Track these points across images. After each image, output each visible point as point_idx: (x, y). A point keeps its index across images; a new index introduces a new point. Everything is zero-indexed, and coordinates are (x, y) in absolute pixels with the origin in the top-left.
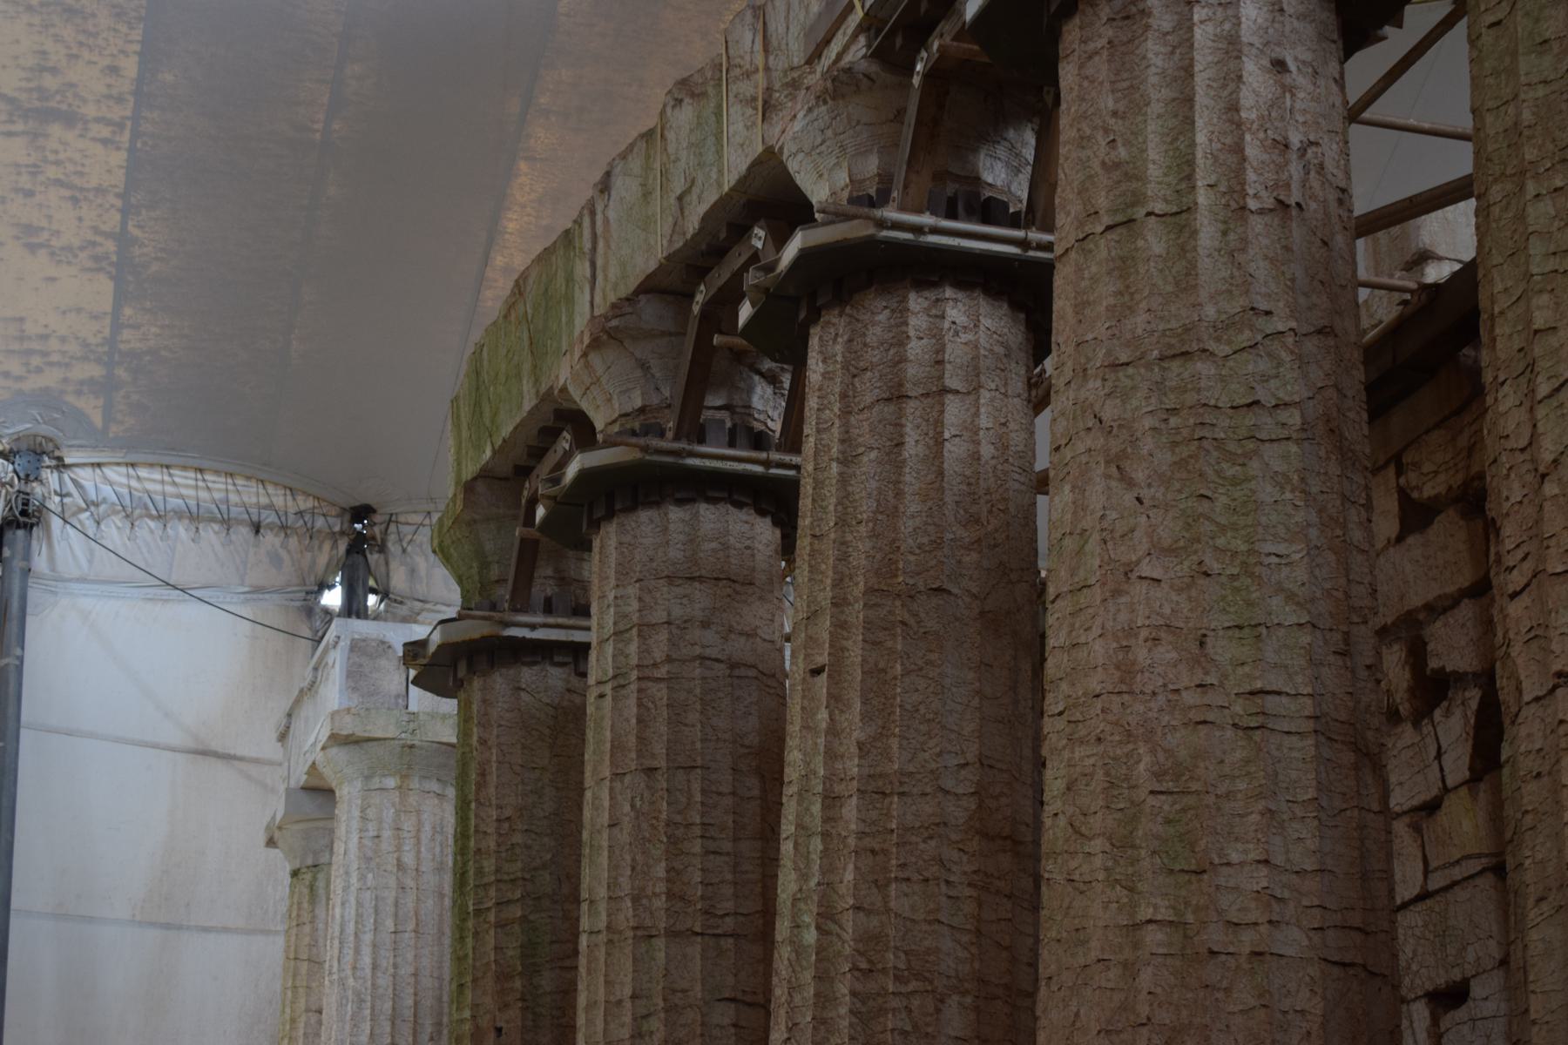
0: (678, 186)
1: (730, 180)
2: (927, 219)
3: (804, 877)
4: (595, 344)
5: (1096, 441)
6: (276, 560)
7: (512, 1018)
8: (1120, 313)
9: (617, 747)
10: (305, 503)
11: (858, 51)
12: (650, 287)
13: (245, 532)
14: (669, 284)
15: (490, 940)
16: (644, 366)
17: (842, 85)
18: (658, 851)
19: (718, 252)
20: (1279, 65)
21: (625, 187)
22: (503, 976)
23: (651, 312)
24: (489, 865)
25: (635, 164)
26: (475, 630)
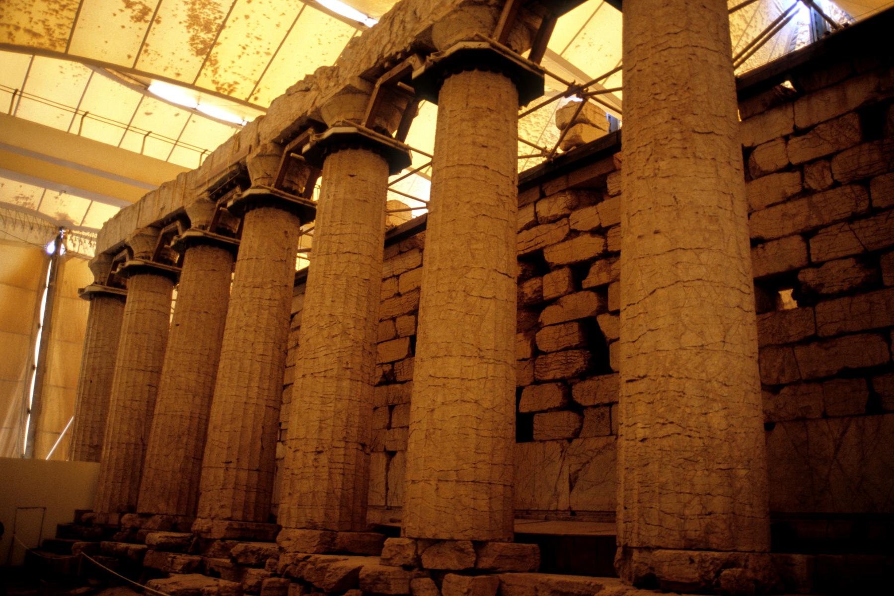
0: (161, 206)
1: (174, 210)
2: (215, 234)
3: (169, 368)
4: (137, 235)
5: (239, 300)
6: (36, 237)
7: (95, 379)
8: (246, 277)
9: (130, 327)
10: (47, 224)
11: (205, 196)
12: (151, 226)
13: (28, 228)
14: (157, 226)
15: (91, 360)
16: (148, 243)
17: (200, 201)
18: (136, 351)
19: (169, 223)
20: (286, 232)
21: (149, 202)
22: (94, 369)
23: (150, 232)
24: (94, 343)
25: (152, 196)
26: (98, 288)
